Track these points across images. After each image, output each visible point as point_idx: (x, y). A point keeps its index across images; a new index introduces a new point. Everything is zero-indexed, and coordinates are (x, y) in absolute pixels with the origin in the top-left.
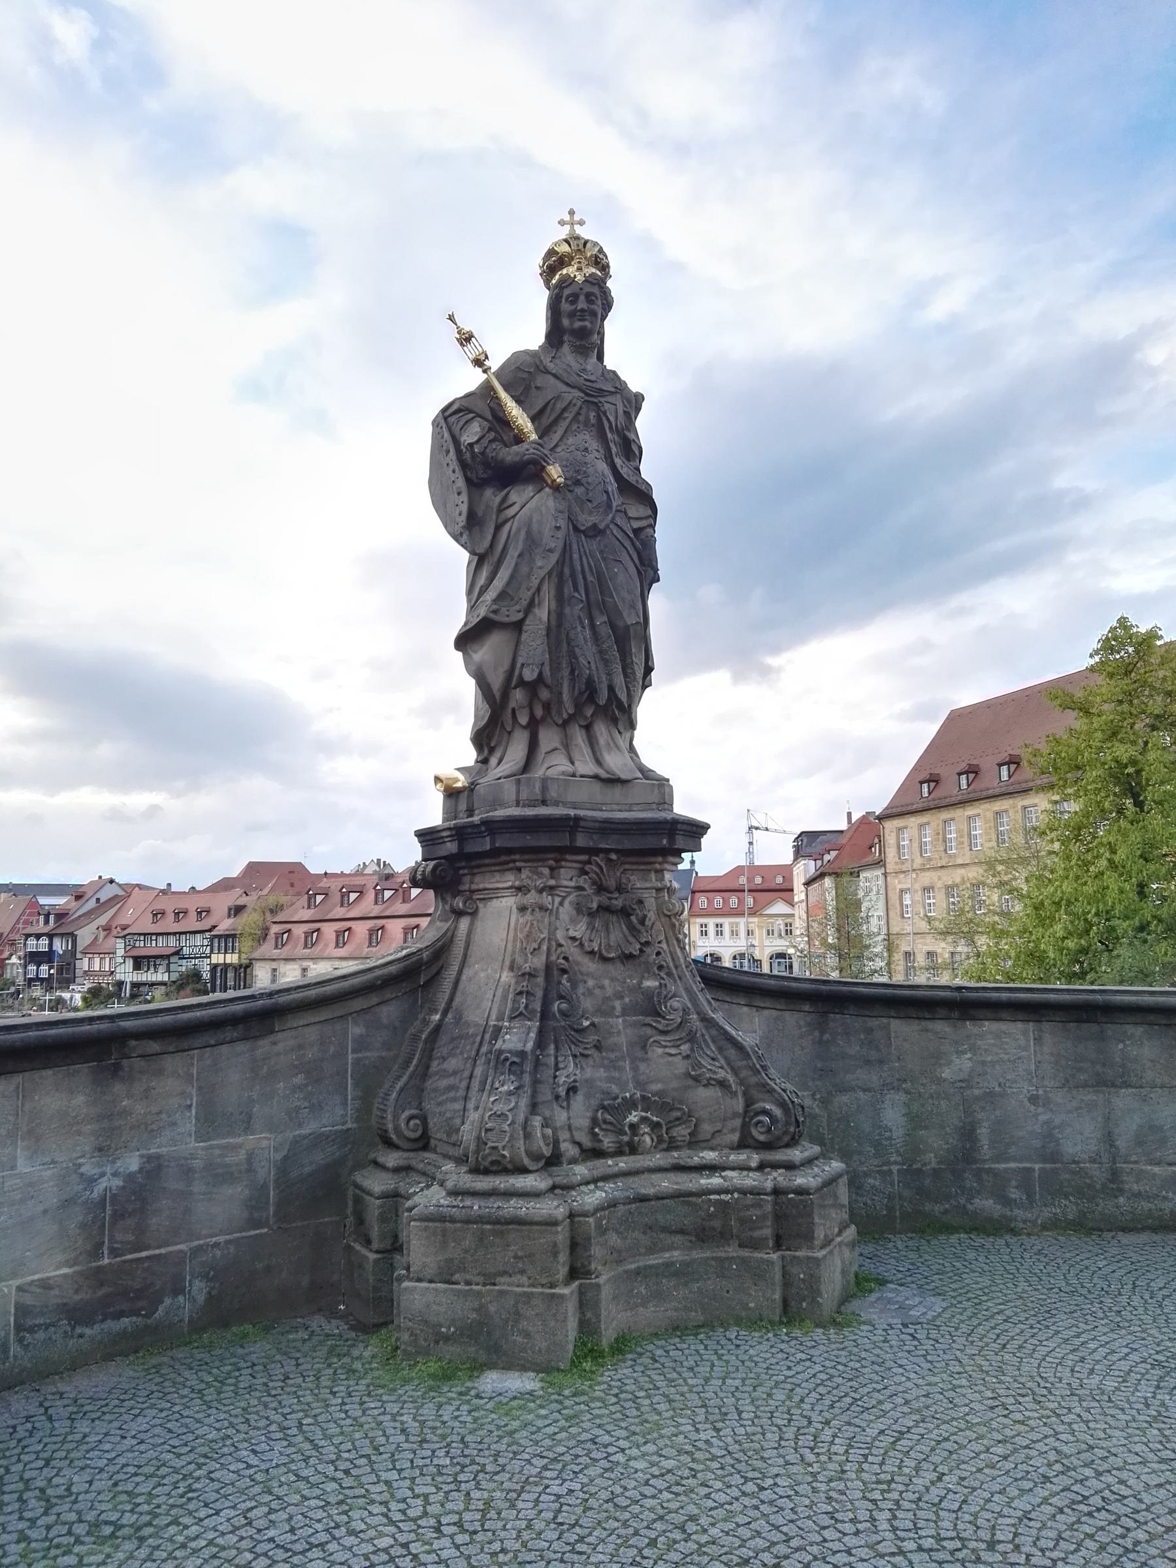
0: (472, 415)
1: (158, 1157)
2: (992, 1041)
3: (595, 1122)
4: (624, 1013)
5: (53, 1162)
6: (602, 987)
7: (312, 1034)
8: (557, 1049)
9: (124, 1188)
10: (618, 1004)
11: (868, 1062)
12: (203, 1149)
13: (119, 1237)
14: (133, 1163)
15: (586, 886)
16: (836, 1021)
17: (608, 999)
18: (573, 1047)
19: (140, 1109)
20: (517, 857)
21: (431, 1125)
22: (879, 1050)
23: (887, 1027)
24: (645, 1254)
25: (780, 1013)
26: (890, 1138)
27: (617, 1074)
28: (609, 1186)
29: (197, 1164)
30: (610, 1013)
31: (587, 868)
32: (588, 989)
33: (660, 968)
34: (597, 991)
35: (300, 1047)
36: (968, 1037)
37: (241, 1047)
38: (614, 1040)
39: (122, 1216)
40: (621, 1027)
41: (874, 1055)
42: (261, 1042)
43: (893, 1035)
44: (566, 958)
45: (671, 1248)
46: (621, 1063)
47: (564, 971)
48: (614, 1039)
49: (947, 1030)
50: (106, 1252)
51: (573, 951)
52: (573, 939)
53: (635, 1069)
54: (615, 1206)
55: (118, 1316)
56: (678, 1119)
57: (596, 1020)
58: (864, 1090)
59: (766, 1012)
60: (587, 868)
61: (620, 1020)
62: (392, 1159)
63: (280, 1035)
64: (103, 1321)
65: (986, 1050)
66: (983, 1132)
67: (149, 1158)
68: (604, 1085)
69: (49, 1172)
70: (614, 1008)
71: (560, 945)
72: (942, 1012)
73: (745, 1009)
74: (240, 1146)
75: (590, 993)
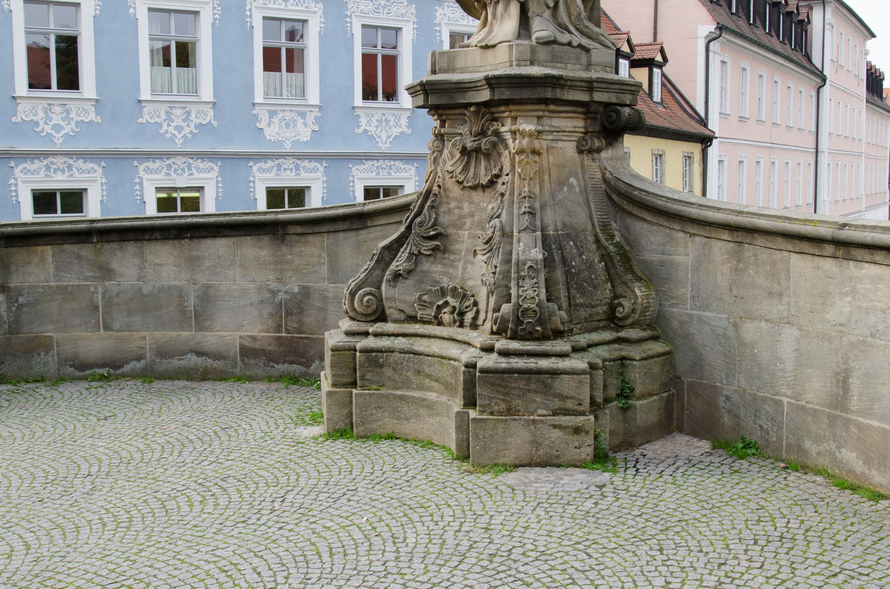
1: (308, 288)
2: (869, 286)
5: (254, 281)
9: (291, 300)
11: (770, 294)
12: (332, 287)
16: (749, 251)
17: (464, 217)
18: (414, 248)
19: (297, 261)
22: (779, 284)
23: (788, 261)
24: (416, 389)
25: (708, 240)
26: (783, 370)
27: (451, 270)
29: (330, 295)
32: (450, 210)
34: (456, 211)
36: (850, 278)
38: (458, 246)
39: (291, 314)
40: (466, 237)
41: (775, 288)
42: (361, 232)
43: (792, 269)
44: (439, 186)
45: (430, 389)
46: (456, 263)
48: (458, 246)
49: (834, 269)
50: (284, 330)
53: (464, 269)
54: (393, 352)
55: (291, 363)
56: (470, 306)
58: (767, 321)
59: (697, 239)
61: (467, 232)
63: (372, 229)
64: (283, 363)
65: (863, 295)
66: (854, 382)
67: (304, 287)
68: (437, 277)
69: (252, 286)
70: (465, 223)
71: (439, 177)
72: (829, 249)
73: (681, 234)
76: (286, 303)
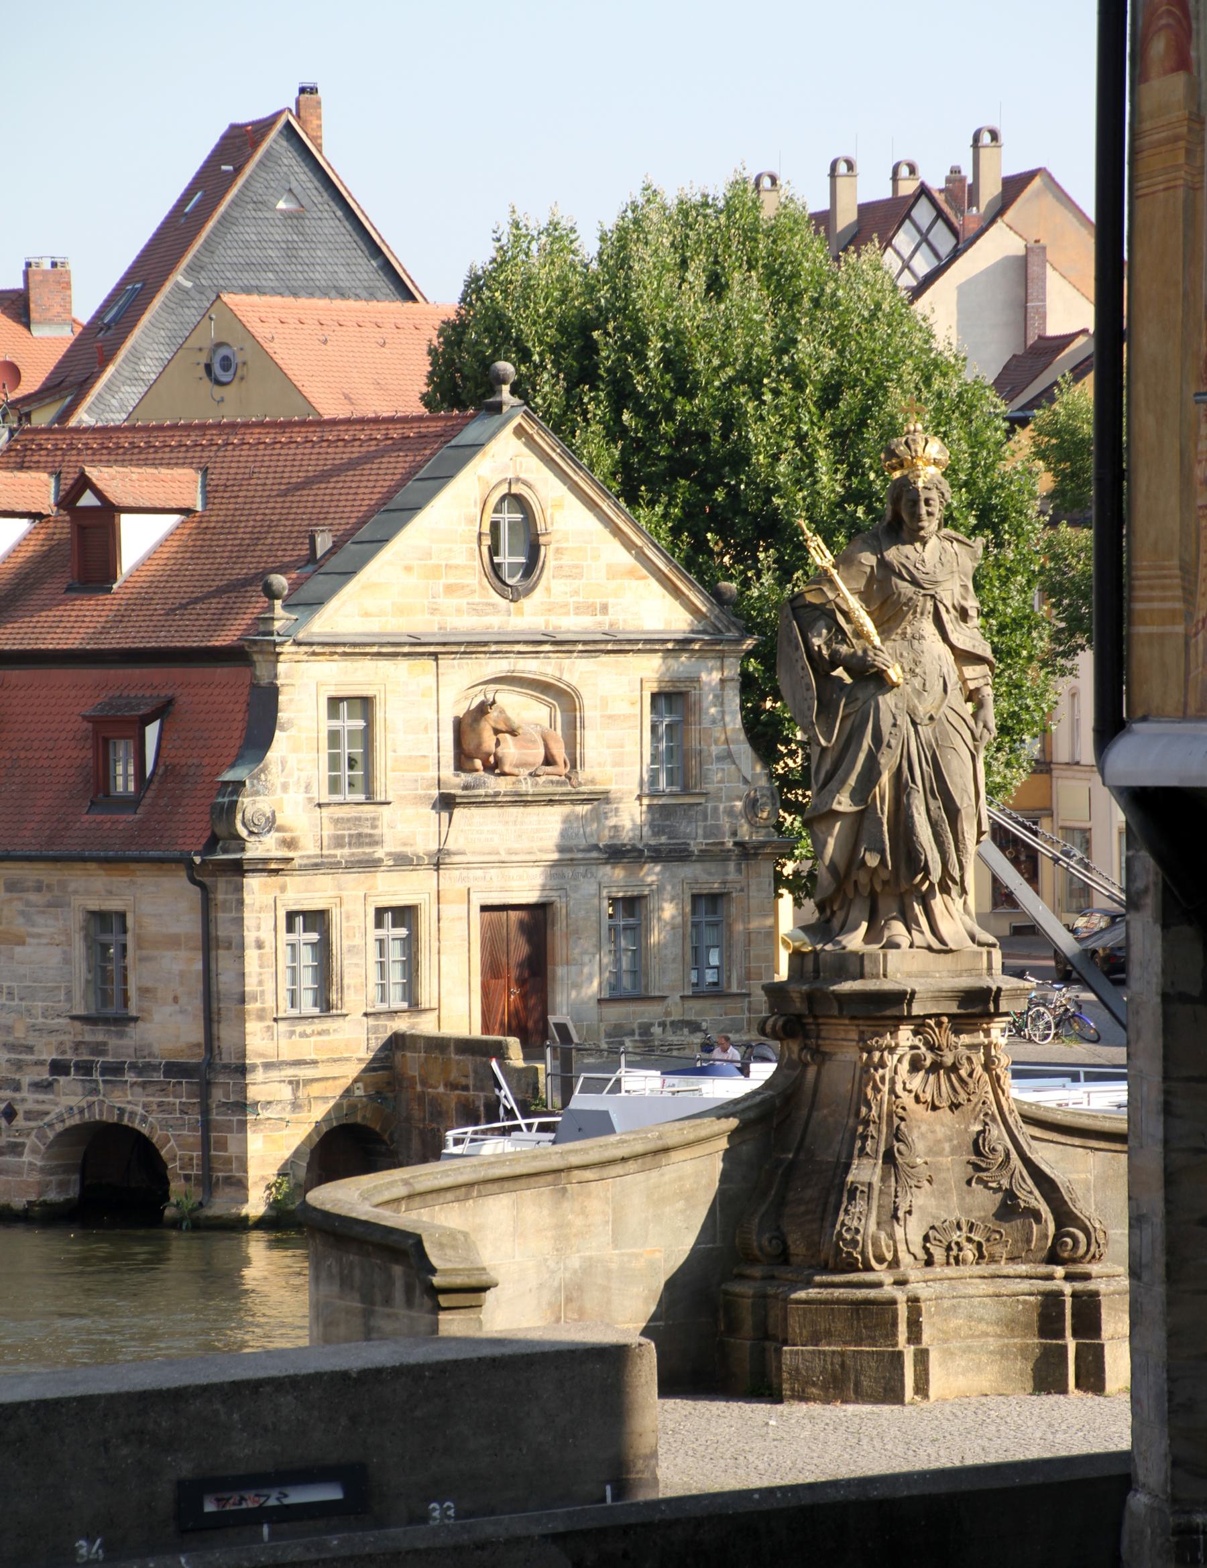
0: (818, 613)
3: (926, 1238)
4: (954, 1151)
6: (933, 1132)
7: (689, 1168)
8: (897, 1181)
10: (947, 1146)
13: (570, 1315)
14: (575, 1262)
15: (921, 1045)
17: (939, 1141)
20: (861, 1022)
21: (790, 1242)
28: (937, 1285)
29: (614, 1266)
30: (940, 1153)
31: (921, 1030)
32: (922, 1134)
33: (986, 1114)
34: (929, 1135)
35: (681, 1178)
37: (640, 1177)
47: (902, 1119)
48: (943, 1175)
51: (907, 1100)
52: (910, 1091)
57: (928, 1160)
60: (921, 1030)
62: (757, 1271)
74: (641, 1255)
75: (923, 1136)
76: (566, 1286)
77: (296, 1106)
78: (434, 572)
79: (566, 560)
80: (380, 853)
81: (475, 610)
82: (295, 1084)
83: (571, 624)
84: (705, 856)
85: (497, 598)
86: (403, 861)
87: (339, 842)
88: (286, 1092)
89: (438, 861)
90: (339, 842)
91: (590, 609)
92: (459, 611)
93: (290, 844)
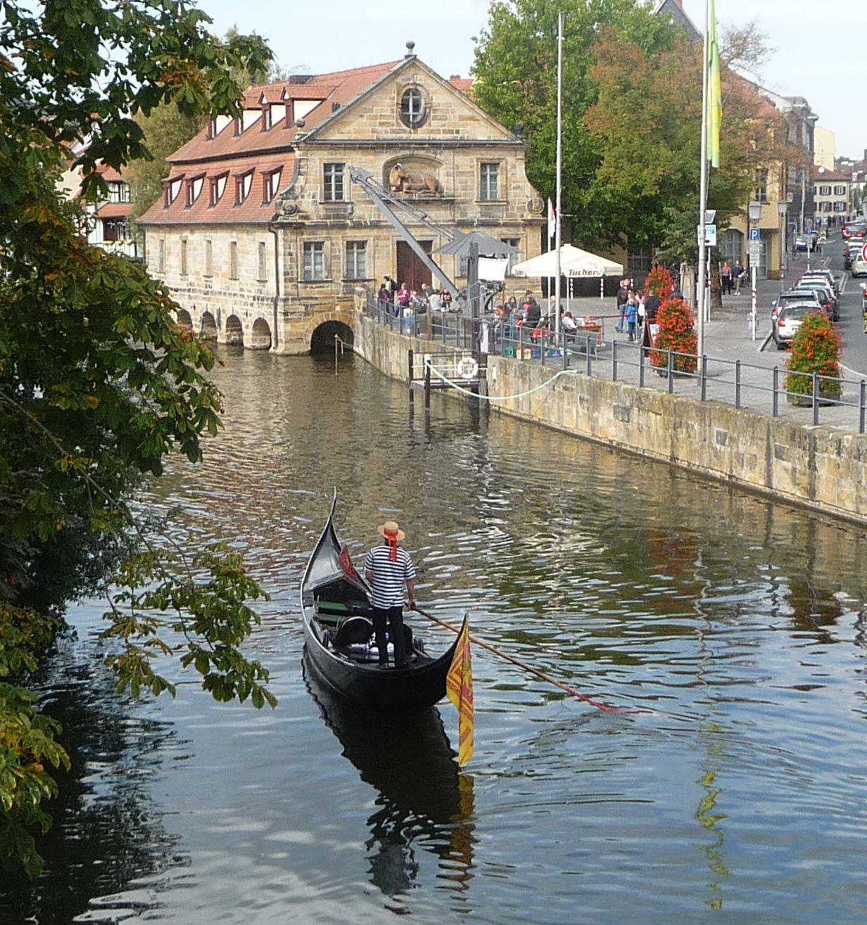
77: (306, 314)
78: (375, 117)
79: (438, 114)
80: (348, 222)
81: (393, 131)
82: (306, 306)
83: (441, 137)
84: (505, 225)
85: (405, 127)
86: (358, 226)
87: (328, 217)
88: (302, 309)
89: (375, 225)
90: (328, 217)
91: (452, 132)
92: (386, 132)
93: (307, 218)
